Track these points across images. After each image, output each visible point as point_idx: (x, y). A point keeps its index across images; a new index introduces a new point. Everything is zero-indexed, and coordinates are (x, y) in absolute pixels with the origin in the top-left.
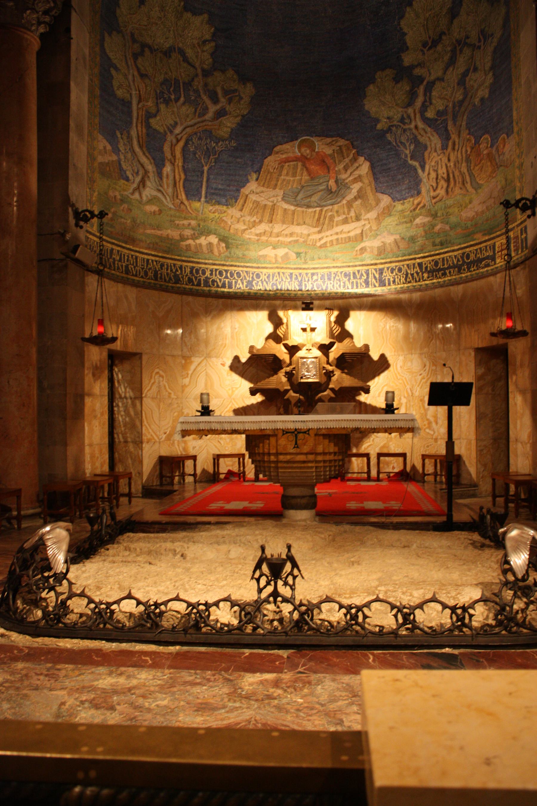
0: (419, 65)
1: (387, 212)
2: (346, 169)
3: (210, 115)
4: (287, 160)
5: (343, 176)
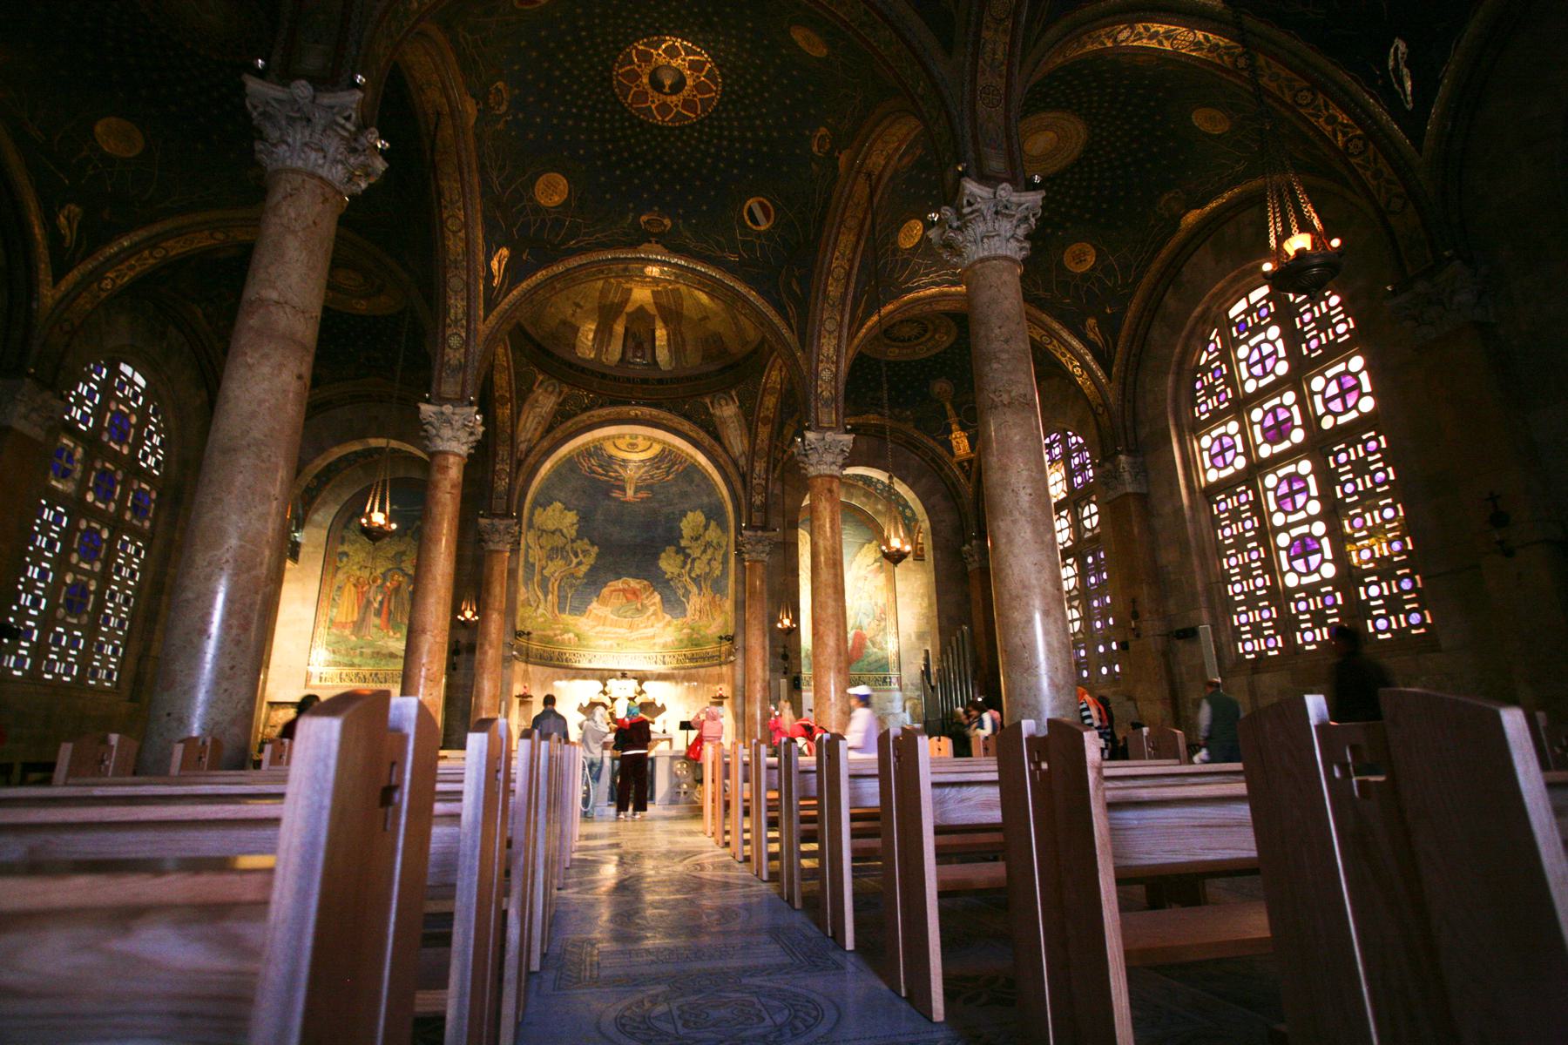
0: (689, 548)
1: (669, 624)
2: (647, 598)
3: (573, 565)
4: (615, 591)
5: (645, 602)
